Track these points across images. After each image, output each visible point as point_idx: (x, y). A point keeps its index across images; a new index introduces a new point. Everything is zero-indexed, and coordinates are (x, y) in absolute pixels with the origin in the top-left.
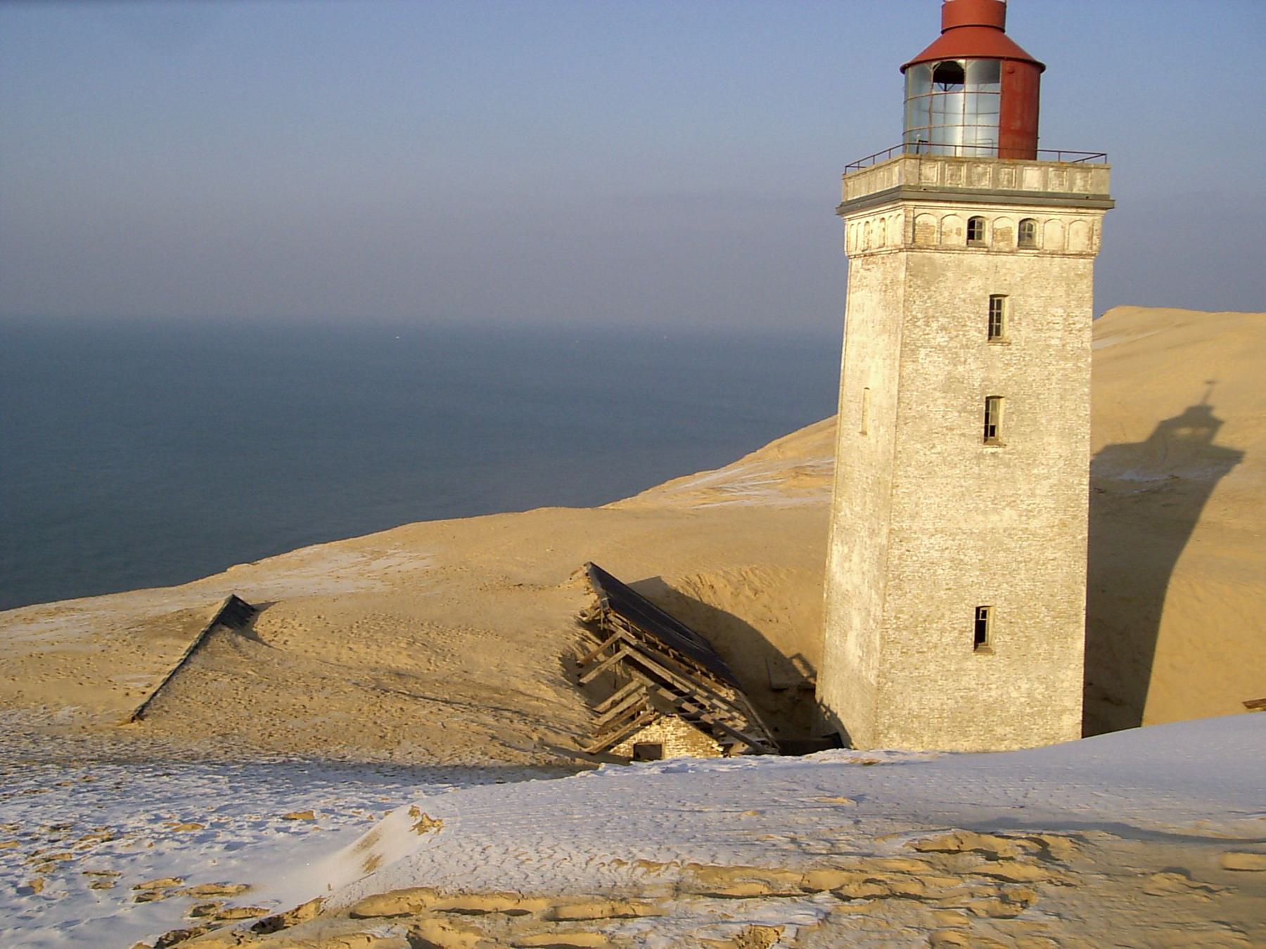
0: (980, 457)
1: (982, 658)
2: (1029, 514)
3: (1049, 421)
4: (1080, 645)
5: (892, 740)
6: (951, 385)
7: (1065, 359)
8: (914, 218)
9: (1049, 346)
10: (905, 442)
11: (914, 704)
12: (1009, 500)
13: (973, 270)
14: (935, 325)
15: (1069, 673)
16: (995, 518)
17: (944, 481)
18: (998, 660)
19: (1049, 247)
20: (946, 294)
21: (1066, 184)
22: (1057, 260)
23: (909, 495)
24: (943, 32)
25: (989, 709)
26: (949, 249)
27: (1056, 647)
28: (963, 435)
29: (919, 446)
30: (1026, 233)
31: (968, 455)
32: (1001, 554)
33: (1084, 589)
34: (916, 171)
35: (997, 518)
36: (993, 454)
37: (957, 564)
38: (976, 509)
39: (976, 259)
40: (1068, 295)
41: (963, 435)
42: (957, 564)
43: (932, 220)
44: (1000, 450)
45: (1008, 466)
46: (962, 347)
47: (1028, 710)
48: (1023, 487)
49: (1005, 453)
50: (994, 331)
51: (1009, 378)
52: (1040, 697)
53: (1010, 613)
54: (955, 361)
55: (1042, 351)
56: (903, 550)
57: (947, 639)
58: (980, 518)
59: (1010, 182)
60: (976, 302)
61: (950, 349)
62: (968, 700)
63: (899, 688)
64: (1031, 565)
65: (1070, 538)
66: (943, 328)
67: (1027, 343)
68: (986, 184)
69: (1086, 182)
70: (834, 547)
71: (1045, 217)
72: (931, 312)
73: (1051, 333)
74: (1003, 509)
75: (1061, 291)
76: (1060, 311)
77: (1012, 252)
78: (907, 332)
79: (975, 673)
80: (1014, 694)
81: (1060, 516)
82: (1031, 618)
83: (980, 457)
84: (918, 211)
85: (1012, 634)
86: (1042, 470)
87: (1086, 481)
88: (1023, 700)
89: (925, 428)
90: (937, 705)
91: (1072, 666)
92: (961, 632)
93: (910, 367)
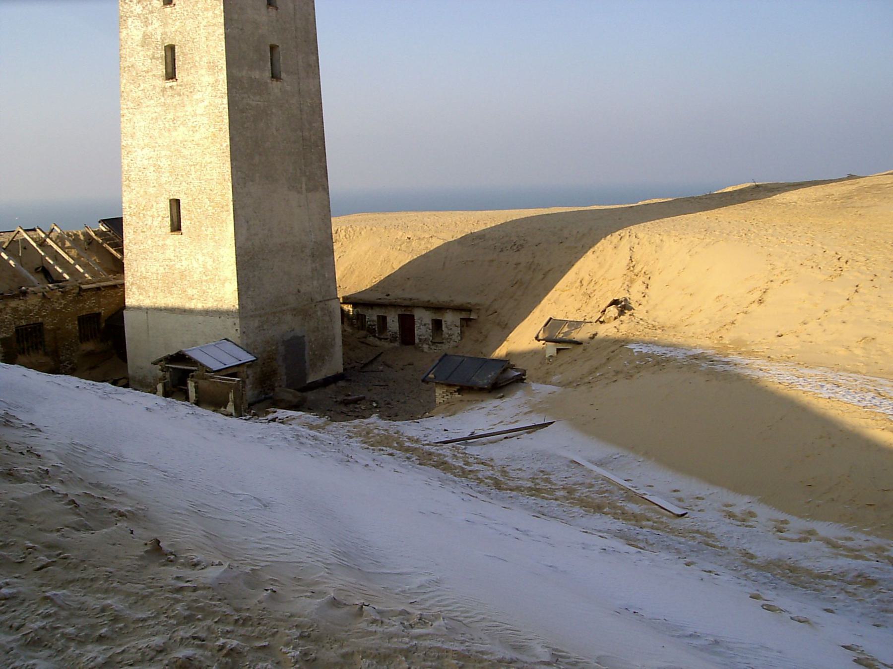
0: (164, 90)
1: (176, 236)
6: (146, 41)
10: (125, 85)
11: (143, 269)
12: (182, 119)
16: (174, 134)
17: (146, 109)
25: (182, 275)
27: (217, 229)
28: (154, 75)
29: (132, 86)
32: (180, 161)
33: (230, 185)
36: (171, 87)
37: (158, 169)
42: (158, 169)
44: (174, 84)
47: (204, 278)
52: (210, 268)
53: (188, 204)
54: (146, 23)
62: (170, 267)
64: (198, 167)
65: (219, 146)
79: (172, 248)
80: (195, 265)
81: (212, 129)
87: (225, 101)
88: (201, 269)
90: (154, 270)
92: (163, 218)
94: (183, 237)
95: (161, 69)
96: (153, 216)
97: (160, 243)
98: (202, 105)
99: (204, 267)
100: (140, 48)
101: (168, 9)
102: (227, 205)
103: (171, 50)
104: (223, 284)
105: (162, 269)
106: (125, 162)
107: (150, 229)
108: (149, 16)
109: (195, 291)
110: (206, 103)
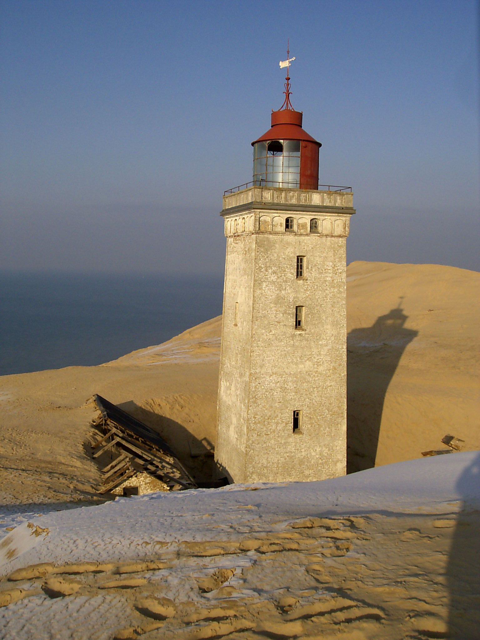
0: (293, 336)
1: (297, 436)
2: (318, 364)
3: (327, 318)
4: (344, 428)
5: (254, 479)
6: (279, 300)
7: (334, 287)
8: (259, 218)
9: (326, 281)
10: (257, 329)
11: (264, 461)
13: (288, 243)
14: (270, 271)
15: (340, 442)
16: (301, 366)
18: (305, 437)
19: (325, 232)
20: (276, 255)
21: (333, 202)
22: (329, 238)
23: (259, 355)
24: (272, 126)
25: (301, 462)
26: (276, 233)
27: (333, 429)
28: (285, 325)
29: (264, 331)
30: (314, 225)
31: (287, 335)
33: (345, 400)
34: (260, 194)
35: (303, 366)
36: (300, 334)
37: (284, 390)
38: (292, 362)
39: (290, 238)
40: (334, 256)
41: (285, 325)
42: (284, 390)
43: (268, 219)
44: (303, 332)
45: (307, 340)
46: (284, 281)
48: (315, 351)
49: (306, 334)
50: (299, 274)
51: (307, 297)
52: (326, 455)
53: (310, 413)
54: (280, 289)
55: (323, 283)
56: (257, 383)
57: (280, 427)
58: (294, 366)
59: (305, 200)
60: (290, 259)
61: (278, 283)
62: (291, 457)
63: (256, 453)
64: (320, 389)
65: (338, 375)
66: (274, 272)
67: (315, 279)
68: (294, 201)
69: (342, 201)
70: (222, 383)
71: (322, 218)
72: (268, 265)
73: (327, 275)
74: (306, 361)
75: (331, 254)
76: (331, 264)
77: (307, 235)
78: (256, 274)
79: (294, 444)
80: (313, 454)
82: (320, 415)
83: (293, 336)
84: (261, 214)
85: (312, 424)
86: (324, 342)
88: (317, 456)
89: (266, 322)
91: (341, 439)
92: (286, 424)
93: (258, 292)
95: (293, 321)
98: (326, 348)
102: (342, 413)
104: (336, 464)
107: (274, 431)
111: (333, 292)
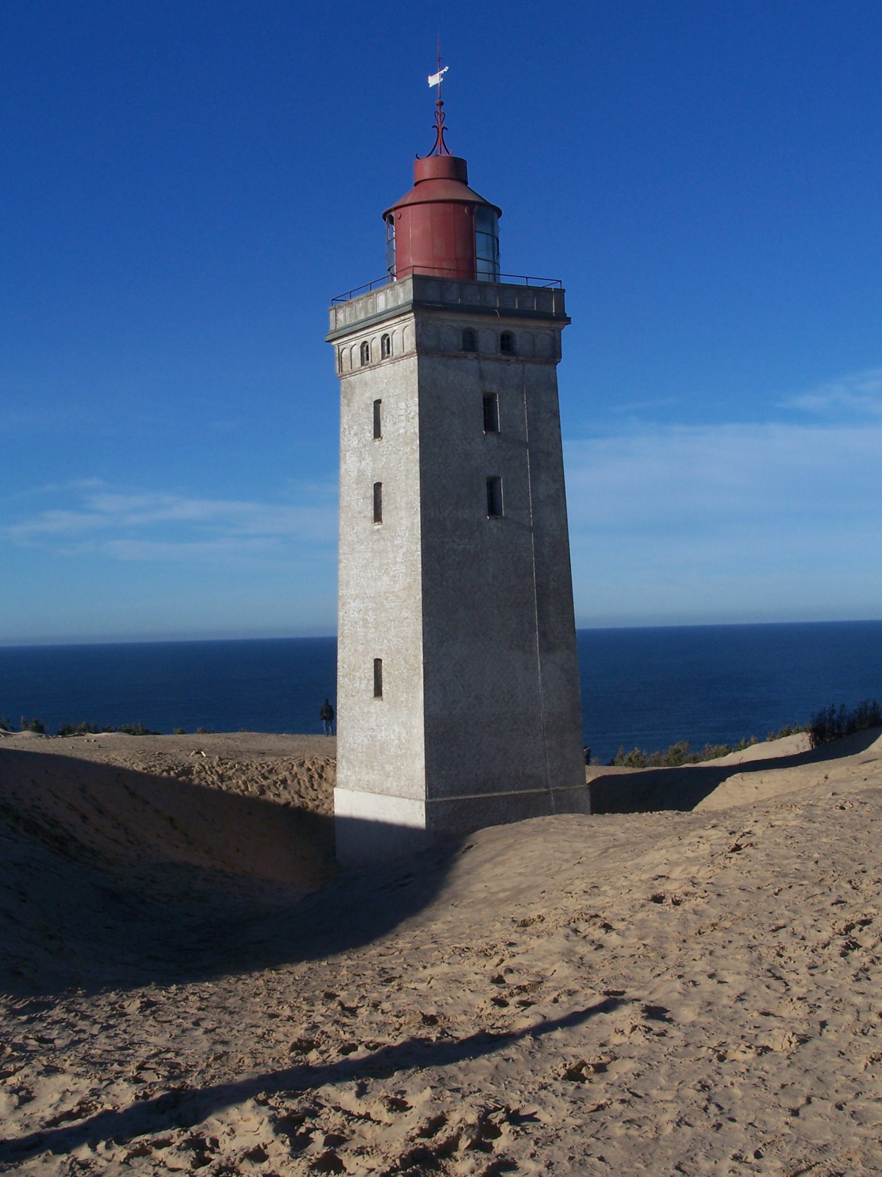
1: (377, 702)
9: (399, 435)
16: (379, 584)
28: (365, 517)
36: (378, 530)
39: (368, 374)
45: (384, 540)
54: (361, 459)
76: (403, 404)
79: (375, 716)
80: (392, 737)
81: (408, 580)
92: (368, 680)
94: (384, 704)
96: (360, 679)
97: (366, 710)
99: (399, 739)
100: (355, 486)
101: (377, 443)
103: (378, 486)
105: (366, 739)
106: (341, 614)
108: (363, 450)
109: (391, 767)
110: (404, 550)
111: (406, 453)
